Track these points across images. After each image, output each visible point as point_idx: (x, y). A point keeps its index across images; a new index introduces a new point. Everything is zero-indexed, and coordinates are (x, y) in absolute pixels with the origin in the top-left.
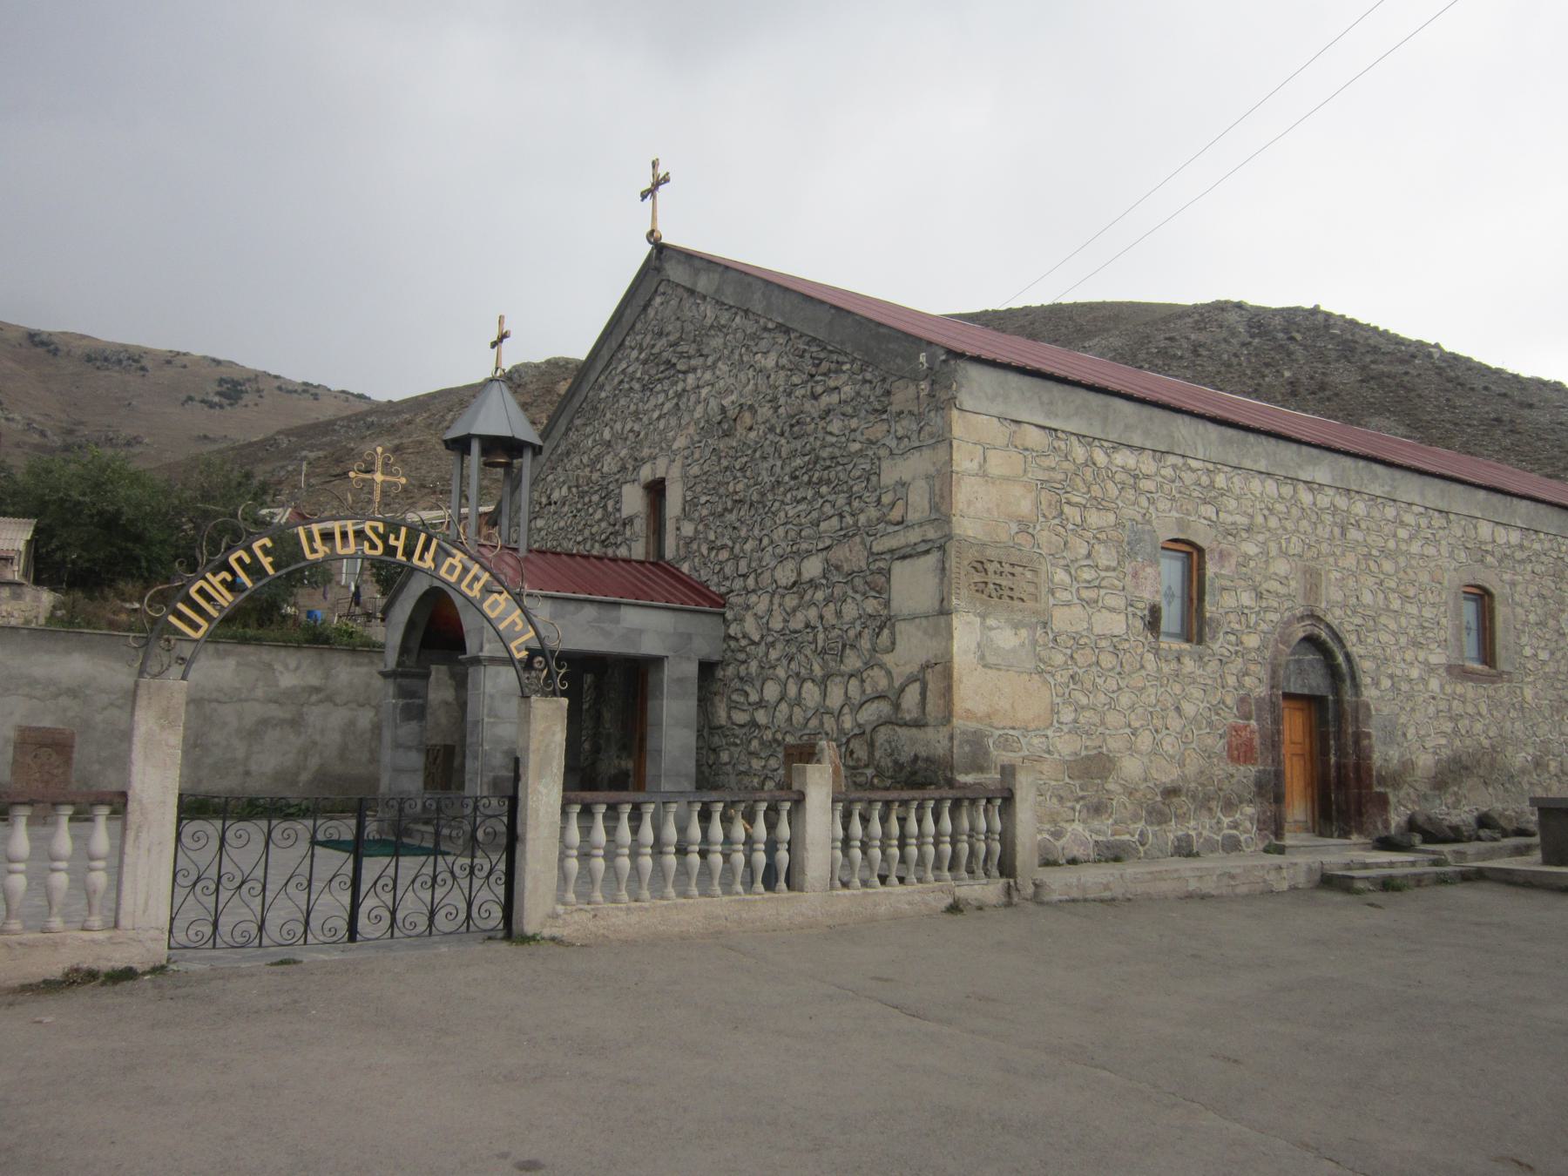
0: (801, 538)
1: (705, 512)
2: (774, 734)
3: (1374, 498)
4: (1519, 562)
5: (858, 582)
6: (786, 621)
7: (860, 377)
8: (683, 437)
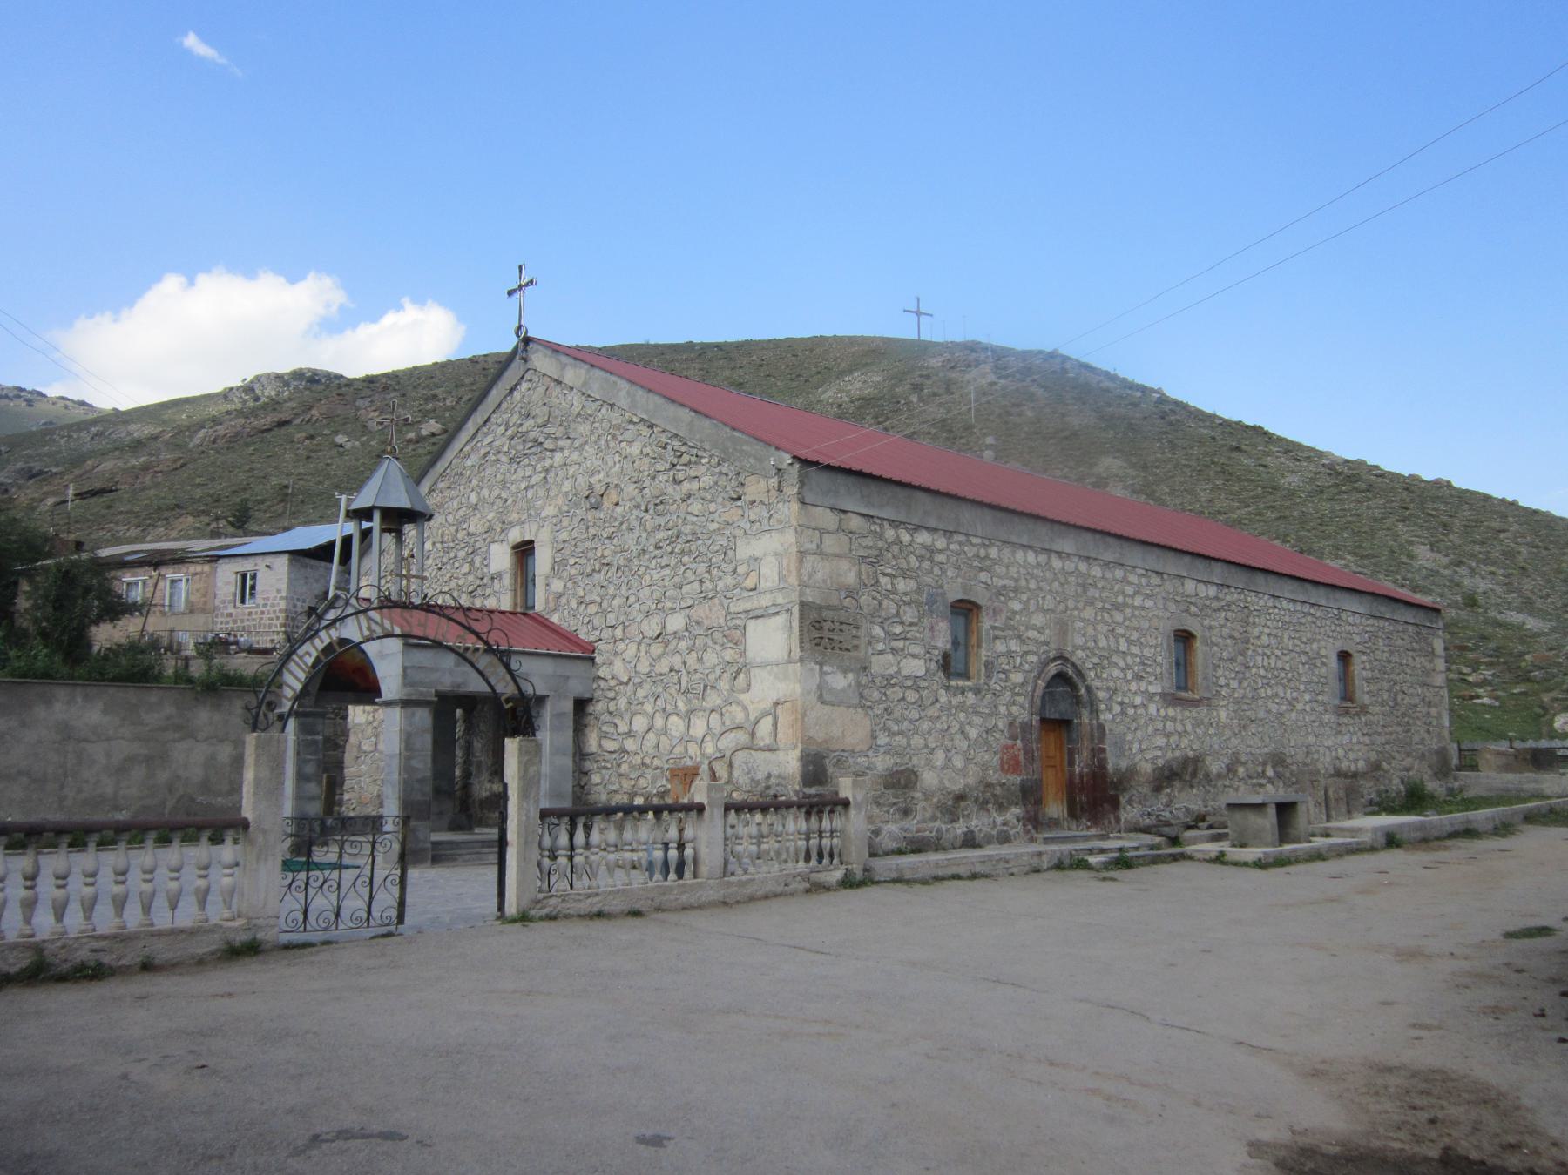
2: (642, 759)
3: (1107, 564)
4: (1215, 610)
6: (651, 665)
7: (717, 470)
8: (552, 507)
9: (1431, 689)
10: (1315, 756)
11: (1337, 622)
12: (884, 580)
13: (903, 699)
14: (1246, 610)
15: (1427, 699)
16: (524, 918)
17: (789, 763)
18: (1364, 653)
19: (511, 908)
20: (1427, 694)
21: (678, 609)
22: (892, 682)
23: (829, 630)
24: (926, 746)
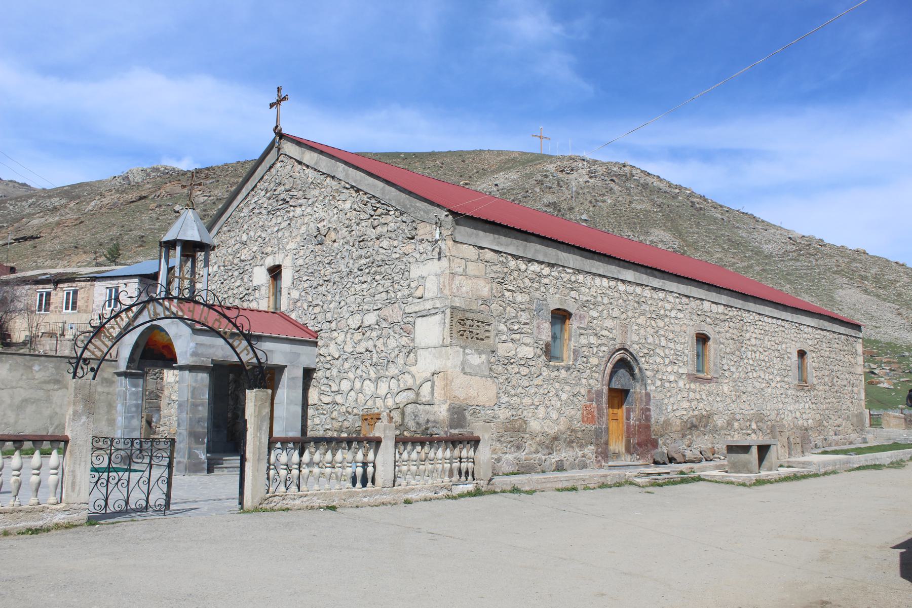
0: (364, 302)
1: (306, 285)
3: (654, 289)
5: (397, 328)
7: (399, 219)
11: (797, 331)
12: (507, 294)
13: (518, 373)
16: (256, 510)
17: (442, 412)
18: (814, 352)
19: (248, 502)
20: (852, 379)
22: (511, 361)
23: (470, 326)
24: (533, 404)
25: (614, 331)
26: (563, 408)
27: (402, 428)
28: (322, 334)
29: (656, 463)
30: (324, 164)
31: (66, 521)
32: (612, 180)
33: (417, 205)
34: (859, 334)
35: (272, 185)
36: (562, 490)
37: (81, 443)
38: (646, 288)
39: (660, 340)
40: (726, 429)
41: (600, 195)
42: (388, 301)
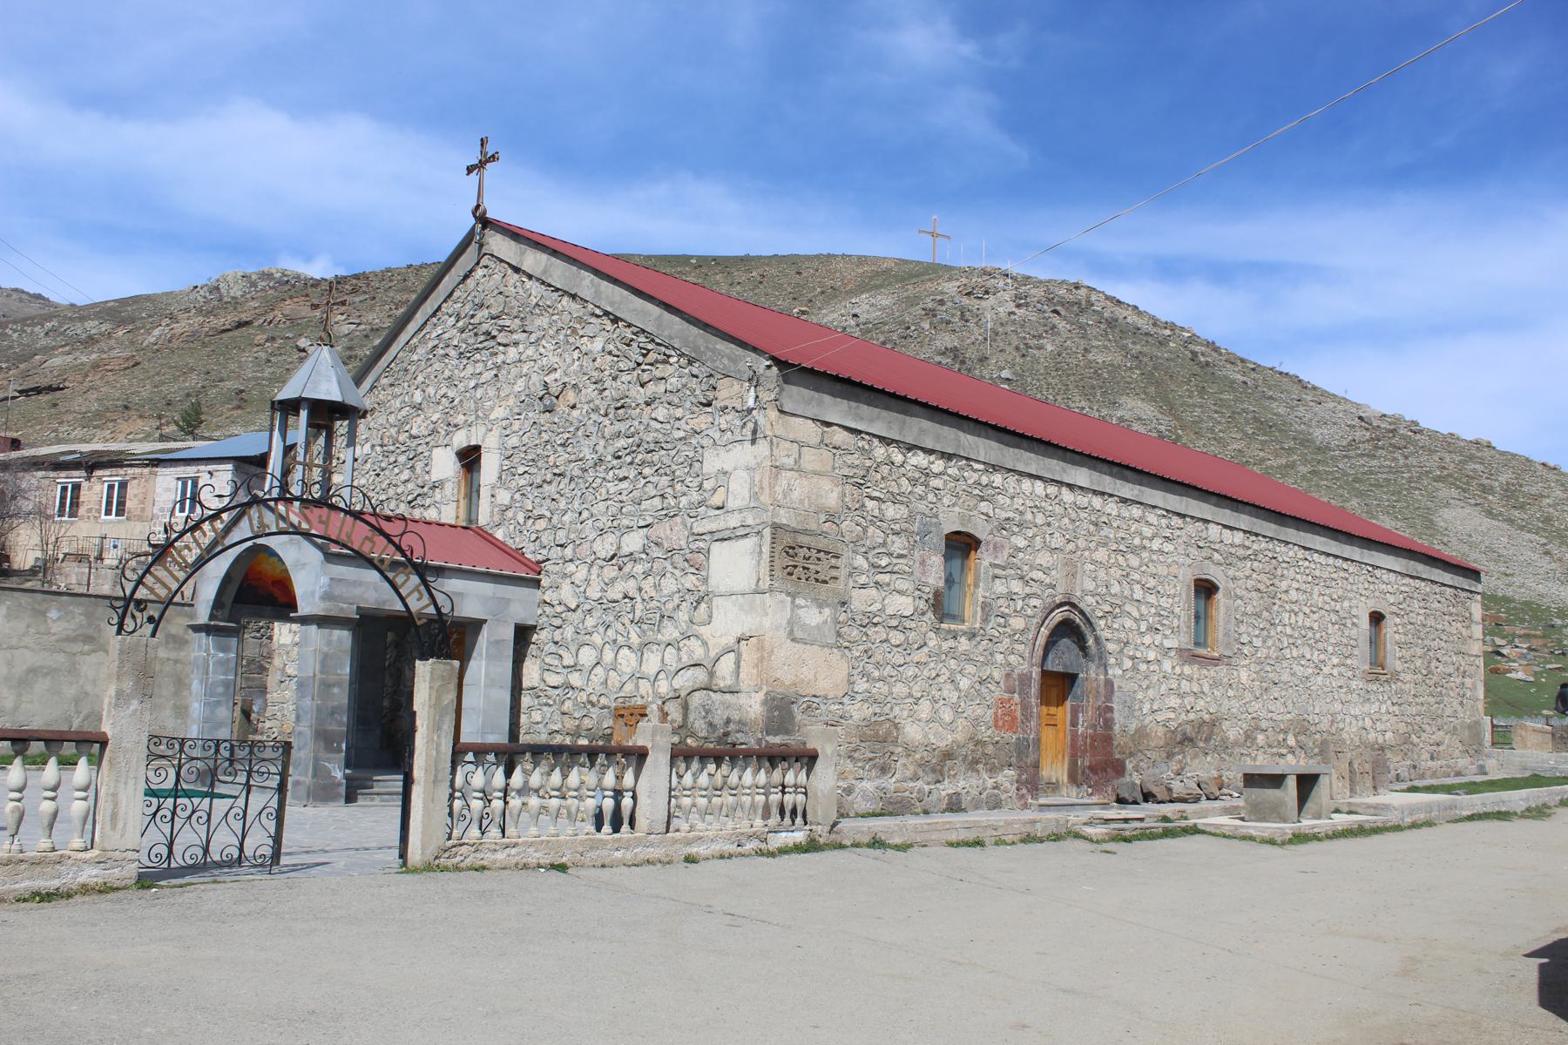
0: (622, 514)
1: (522, 482)
3: (1124, 501)
5: (678, 559)
7: (687, 371)
9: (1467, 658)
10: (1341, 726)
11: (1370, 579)
12: (870, 504)
13: (886, 641)
14: (1274, 561)
15: (1462, 668)
16: (428, 868)
17: (752, 706)
18: (1397, 615)
19: (415, 854)
20: (1463, 664)
21: (635, 528)
22: (875, 621)
23: (804, 558)
24: (910, 695)
25: (1053, 573)
26: (962, 704)
27: (682, 732)
28: (548, 566)
29: (1121, 801)
30: (559, 273)
31: (100, 881)
32: (1055, 312)
33: (718, 347)
34: (1476, 586)
35: (467, 307)
36: (958, 844)
37: (128, 745)
38: (1110, 499)
39: (1132, 590)
40: (1242, 746)
41: (1034, 337)
42: (664, 512)
